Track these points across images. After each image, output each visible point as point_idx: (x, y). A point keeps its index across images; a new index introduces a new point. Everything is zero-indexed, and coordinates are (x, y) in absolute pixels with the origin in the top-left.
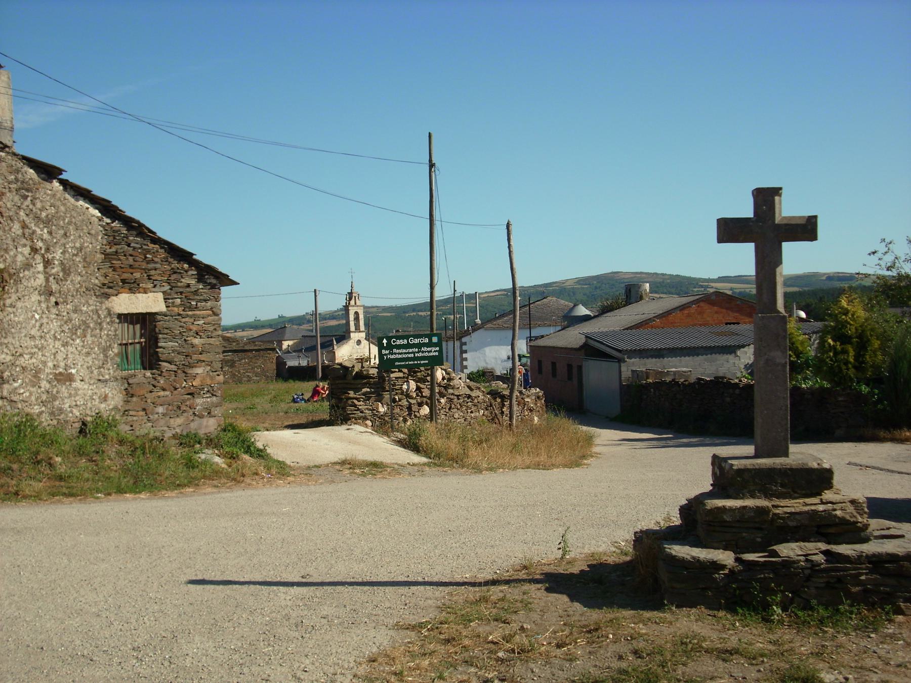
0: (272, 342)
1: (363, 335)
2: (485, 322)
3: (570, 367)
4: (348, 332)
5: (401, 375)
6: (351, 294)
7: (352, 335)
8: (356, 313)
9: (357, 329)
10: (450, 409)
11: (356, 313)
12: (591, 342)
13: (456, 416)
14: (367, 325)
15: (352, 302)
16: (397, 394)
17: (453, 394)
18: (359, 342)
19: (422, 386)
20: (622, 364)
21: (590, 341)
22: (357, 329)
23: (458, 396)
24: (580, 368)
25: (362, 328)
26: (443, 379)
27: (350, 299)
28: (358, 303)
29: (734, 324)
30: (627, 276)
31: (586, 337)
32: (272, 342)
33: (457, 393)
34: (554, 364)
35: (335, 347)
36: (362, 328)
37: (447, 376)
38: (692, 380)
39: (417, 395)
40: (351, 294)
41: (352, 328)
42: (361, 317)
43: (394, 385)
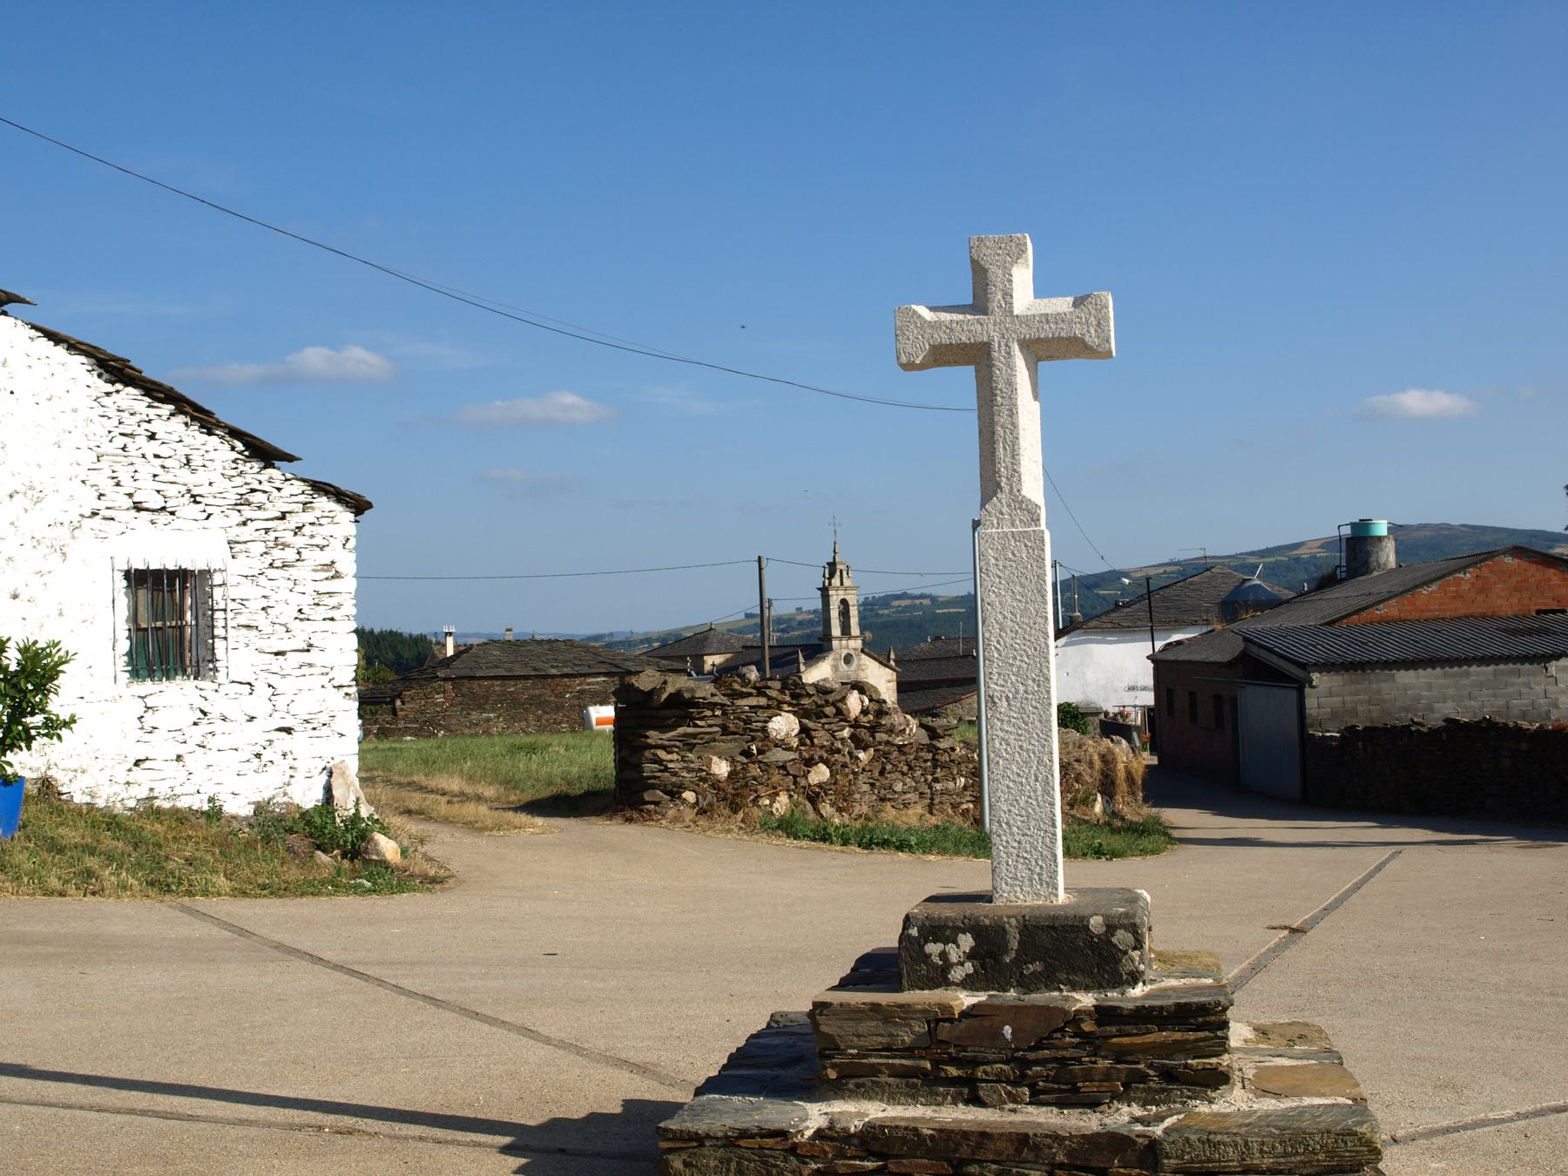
0: (683, 659)
1: (858, 644)
2: (1088, 618)
3: (1218, 699)
4: (827, 637)
5: (763, 701)
6: (832, 566)
7: (835, 643)
8: (844, 602)
9: (846, 630)
10: (882, 773)
11: (844, 602)
12: (1255, 649)
13: (899, 787)
14: (863, 628)
15: (836, 581)
16: (753, 739)
17: (887, 743)
18: (848, 659)
19: (810, 724)
20: (1307, 690)
21: (1255, 649)
22: (846, 630)
23: (900, 748)
24: (1234, 700)
25: (855, 631)
26: (865, 712)
27: (832, 575)
28: (847, 582)
29: (1554, 612)
30: (1422, 534)
31: (1245, 639)
32: (683, 659)
33: (899, 741)
34: (1192, 694)
35: (802, 668)
36: (855, 631)
37: (874, 706)
38: (1435, 720)
39: (802, 743)
40: (832, 566)
41: (836, 631)
42: (854, 612)
43: (748, 721)
